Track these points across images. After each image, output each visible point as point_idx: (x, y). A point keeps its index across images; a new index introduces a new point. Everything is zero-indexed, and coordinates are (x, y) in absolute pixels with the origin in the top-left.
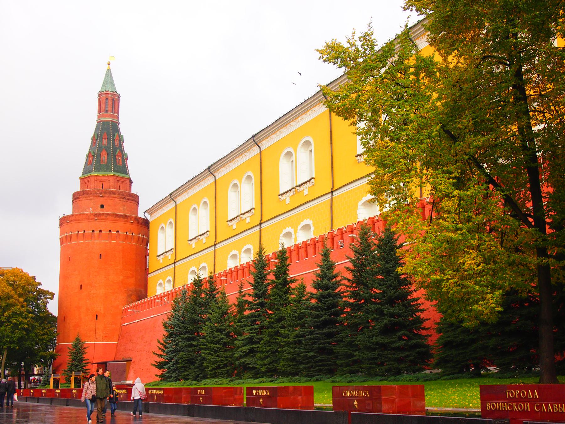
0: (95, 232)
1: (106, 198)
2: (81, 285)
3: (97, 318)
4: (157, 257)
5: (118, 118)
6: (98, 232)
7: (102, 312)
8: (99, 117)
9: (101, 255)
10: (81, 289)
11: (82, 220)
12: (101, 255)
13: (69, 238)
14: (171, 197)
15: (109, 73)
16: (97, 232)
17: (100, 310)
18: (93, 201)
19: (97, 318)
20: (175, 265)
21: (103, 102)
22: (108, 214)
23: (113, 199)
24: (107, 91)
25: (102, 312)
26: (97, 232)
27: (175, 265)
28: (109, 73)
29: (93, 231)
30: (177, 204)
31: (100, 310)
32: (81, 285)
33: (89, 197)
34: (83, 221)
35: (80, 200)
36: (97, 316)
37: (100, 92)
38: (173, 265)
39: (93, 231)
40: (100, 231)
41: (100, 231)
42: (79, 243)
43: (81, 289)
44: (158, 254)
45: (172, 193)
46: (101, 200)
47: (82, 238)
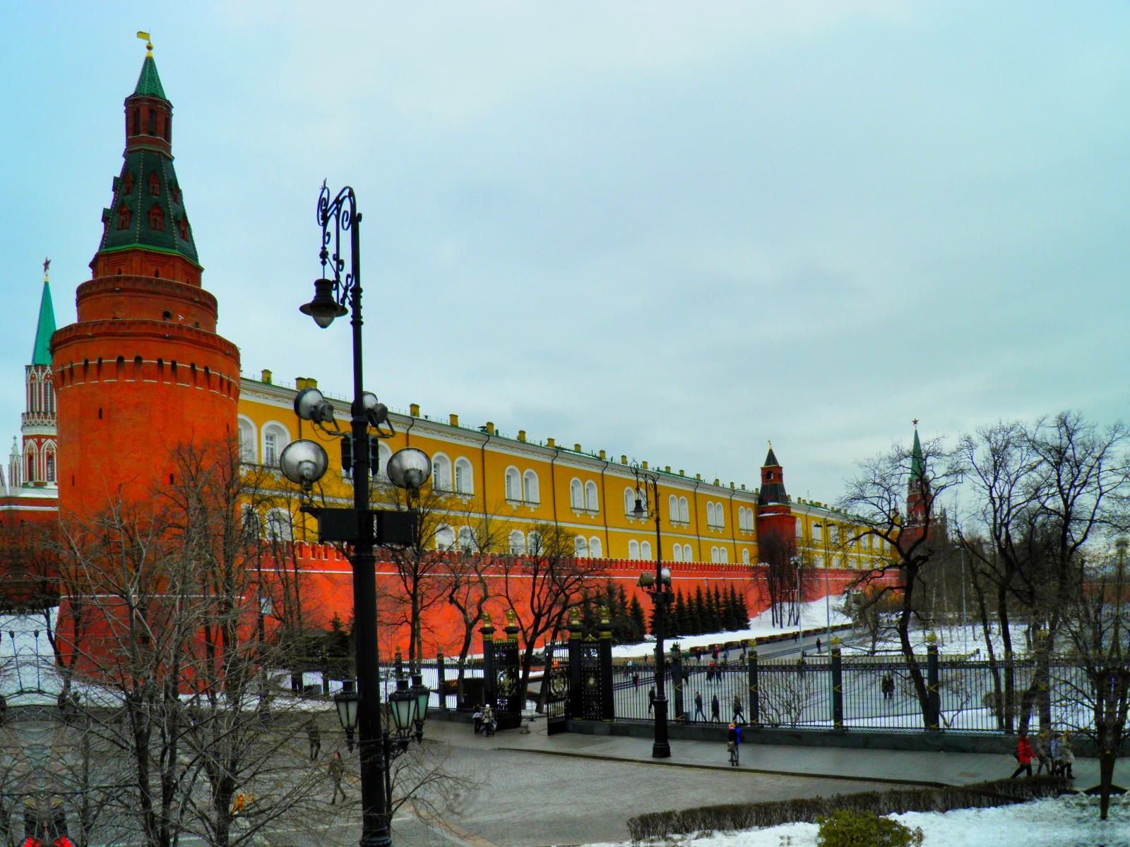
5: (168, 148)
8: (129, 142)
13: (93, 371)
15: (149, 64)
16: (167, 363)
21: (144, 115)
24: (153, 95)
26: (167, 363)
28: (149, 64)
29: (160, 361)
39: (160, 361)
40: (174, 363)
41: (174, 363)
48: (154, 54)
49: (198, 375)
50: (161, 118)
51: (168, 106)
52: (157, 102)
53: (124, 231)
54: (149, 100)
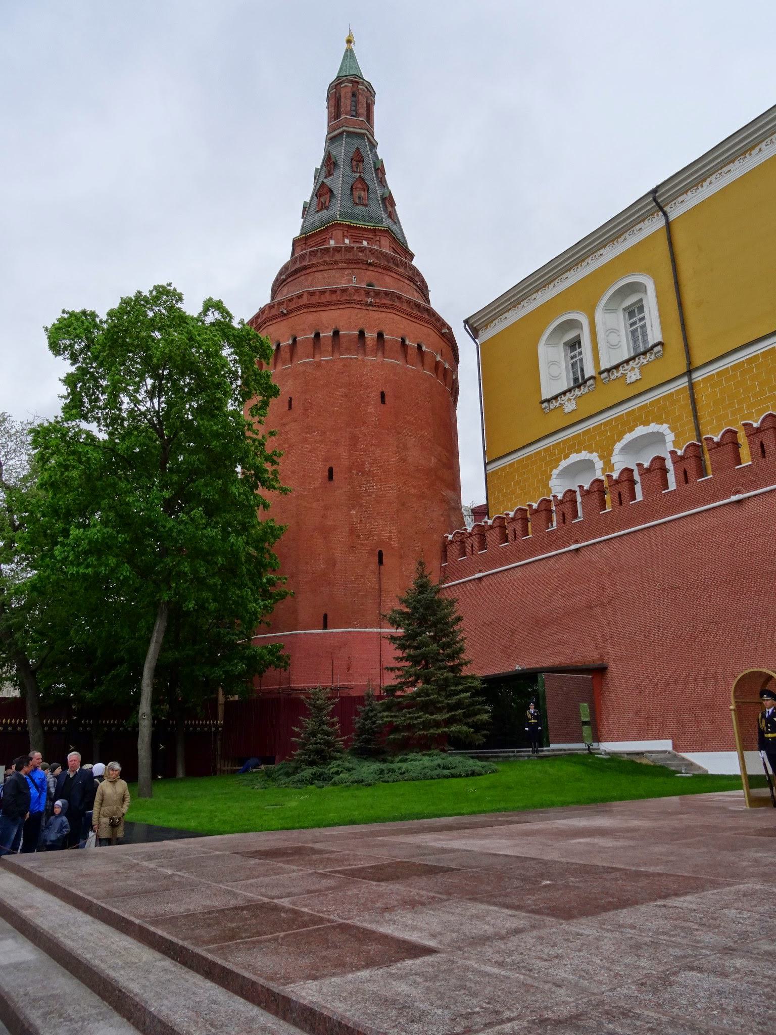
0: (368, 335)
1: (380, 270)
2: (331, 471)
3: (381, 562)
4: (546, 404)
6: (375, 335)
7: (395, 543)
8: (331, 129)
9: (383, 395)
10: (331, 476)
11: (330, 304)
12: (383, 395)
13: (285, 354)
14: (655, 200)
15: (349, 55)
16: (371, 335)
17: (390, 538)
18: (347, 272)
19: (381, 562)
20: (690, 379)
22: (399, 298)
23: (395, 276)
25: (395, 543)
26: (371, 335)
27: (690, 379)
28: (349, 55)
29: (362, 333)
30: (671, 218)
31: (390, 538)
32: (331, 471)
33: (336, 263)
34: (333, 307)
35: (309, 271)
36: (380, 554)
37: (338, 78)
38: (686, 379)
39: (362, 333)
40: (380, 335)
41: (380, 335)
42: (319, 365)
43: (331, 476)
44: (545, 395)
45: (658, 187)
46: (369, 273)
47: (330, 349)
48: (354, 47)
49: (410, 352)
50: (363, 101)
51: (370, 93)
52: (358, 82)
53: (324, 213)
54: (352, 82)
